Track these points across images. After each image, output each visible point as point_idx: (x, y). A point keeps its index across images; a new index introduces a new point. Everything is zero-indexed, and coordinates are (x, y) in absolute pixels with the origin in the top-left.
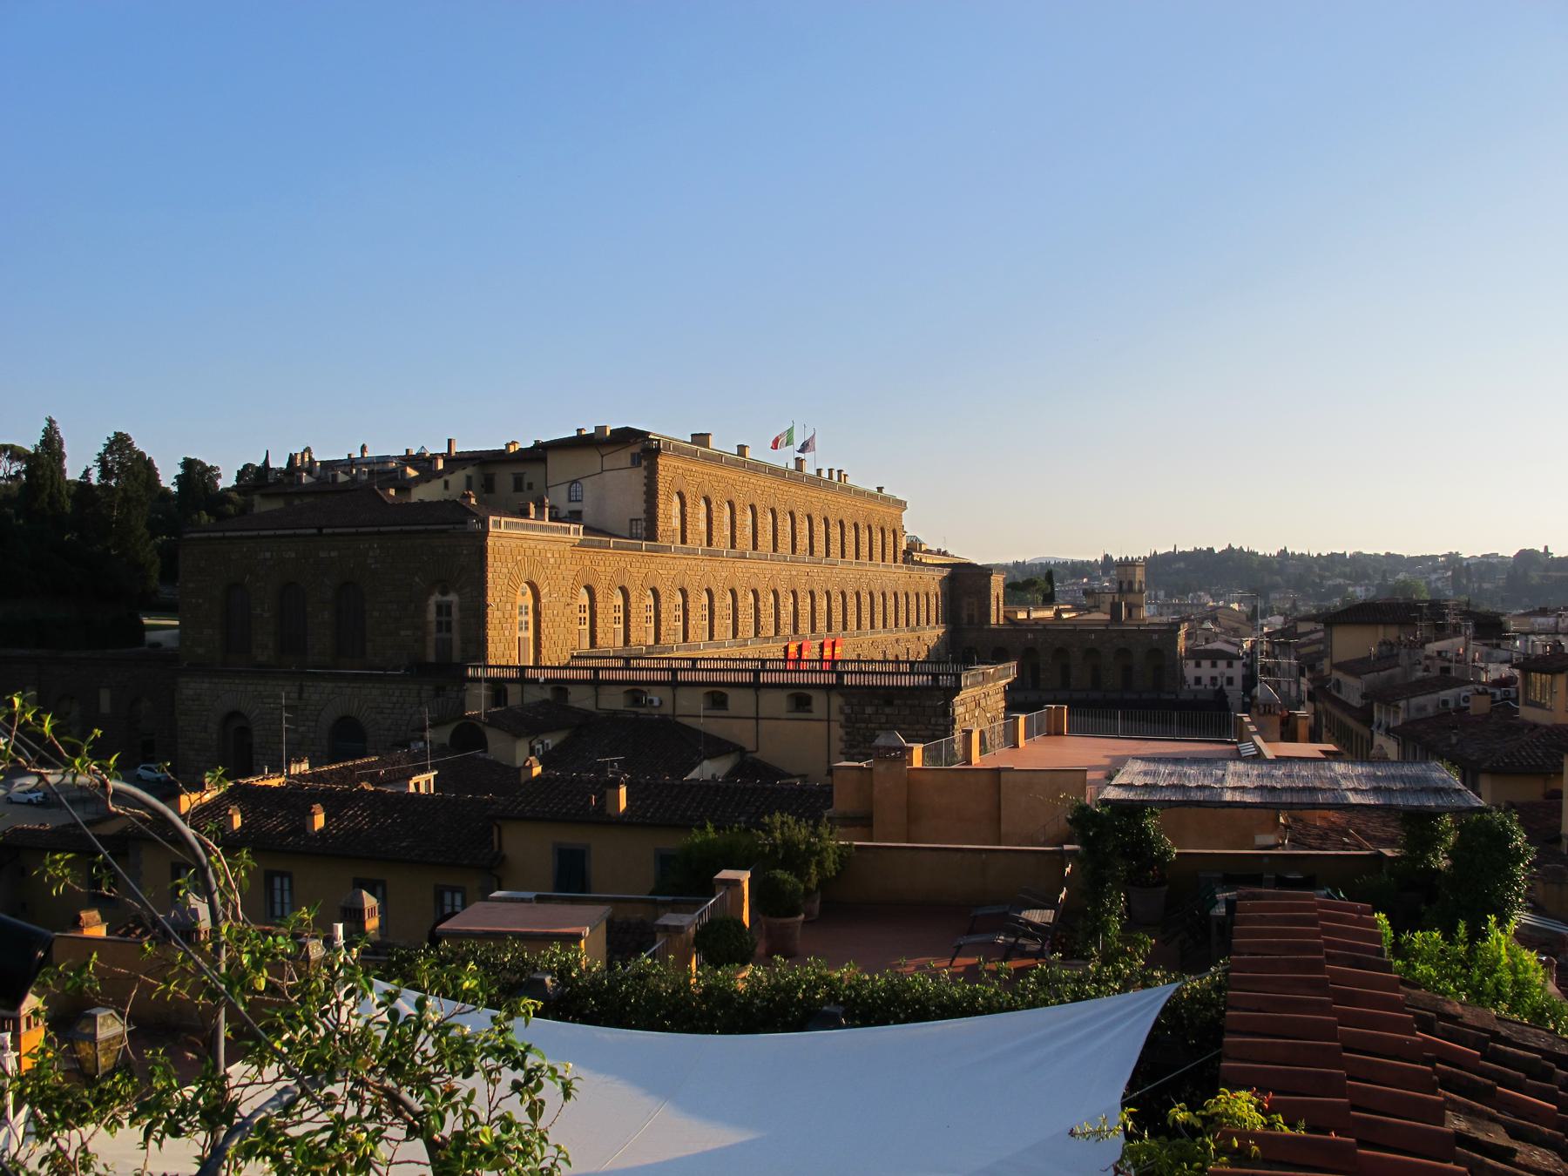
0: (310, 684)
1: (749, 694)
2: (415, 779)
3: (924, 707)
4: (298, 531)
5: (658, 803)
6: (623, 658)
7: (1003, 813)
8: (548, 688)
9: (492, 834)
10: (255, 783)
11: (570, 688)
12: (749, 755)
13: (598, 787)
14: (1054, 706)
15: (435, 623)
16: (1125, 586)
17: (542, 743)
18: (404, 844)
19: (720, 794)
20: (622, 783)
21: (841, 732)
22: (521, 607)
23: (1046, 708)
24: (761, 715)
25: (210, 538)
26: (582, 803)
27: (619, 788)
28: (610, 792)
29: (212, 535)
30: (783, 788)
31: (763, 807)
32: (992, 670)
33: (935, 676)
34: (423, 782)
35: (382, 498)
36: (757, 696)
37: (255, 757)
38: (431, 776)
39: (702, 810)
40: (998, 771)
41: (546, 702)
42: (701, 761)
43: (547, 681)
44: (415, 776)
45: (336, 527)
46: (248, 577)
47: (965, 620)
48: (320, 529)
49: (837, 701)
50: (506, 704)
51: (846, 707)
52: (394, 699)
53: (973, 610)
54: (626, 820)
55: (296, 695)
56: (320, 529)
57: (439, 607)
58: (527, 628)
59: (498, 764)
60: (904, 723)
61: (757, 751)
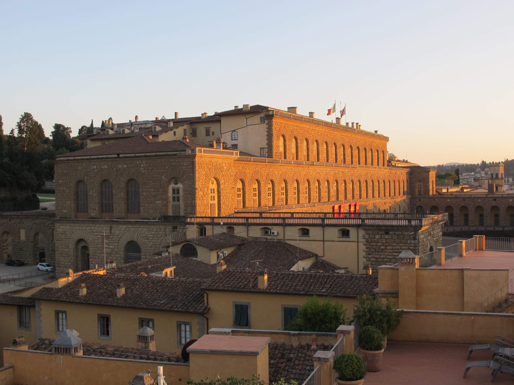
0: (115, 226)
1: (319, 230)
2: (166, 270)
3: (404, 235)
4: (108, 156)
5: (282, 283)
6: (259, 213)
7: (466, 291)
8: (225, 227)
9: (204, 297)
10: (92, 273)
11: (235, 227)
12: (320, 258)
13: (253, 275)
14: (478, 236)
15: (172, 198)
16: (494, 176)
17: (223, 253)
18: (162, 302)
19: (313, 278)
20: (265, 273)
21: (364, 247)
22: (211, 190)
23: (474, 237)
25: (68, 160)
26: (246, 283)
27: (264, 276)
28: (259, 277)
29: (69, 158)
30: (342, 276)
31: (334, 285)
32: (436, 217)
33: (410, 221)
34: (169, 271)
35: (146, 140)
36: (324, 230)
37: (90, 260)
38: (172, 269)
39: (304, 286)
40: (462, 270)
41: (224, 233)
42: (298, 261)
43: (224, 224)
44: (164, 269)
47: (417, 194)
48: (118, 155)
49: (362, 232)
50: (205, 235)
51: (366, 235)
52: (154, 233)
53: (421, 188)
54: (268, 291)
55: (109, 231)
56: (118, 155)
57: (174, 190)
58: (214, 199)
59: (203, 263)
60: (394, 243)
61: (323, 256)
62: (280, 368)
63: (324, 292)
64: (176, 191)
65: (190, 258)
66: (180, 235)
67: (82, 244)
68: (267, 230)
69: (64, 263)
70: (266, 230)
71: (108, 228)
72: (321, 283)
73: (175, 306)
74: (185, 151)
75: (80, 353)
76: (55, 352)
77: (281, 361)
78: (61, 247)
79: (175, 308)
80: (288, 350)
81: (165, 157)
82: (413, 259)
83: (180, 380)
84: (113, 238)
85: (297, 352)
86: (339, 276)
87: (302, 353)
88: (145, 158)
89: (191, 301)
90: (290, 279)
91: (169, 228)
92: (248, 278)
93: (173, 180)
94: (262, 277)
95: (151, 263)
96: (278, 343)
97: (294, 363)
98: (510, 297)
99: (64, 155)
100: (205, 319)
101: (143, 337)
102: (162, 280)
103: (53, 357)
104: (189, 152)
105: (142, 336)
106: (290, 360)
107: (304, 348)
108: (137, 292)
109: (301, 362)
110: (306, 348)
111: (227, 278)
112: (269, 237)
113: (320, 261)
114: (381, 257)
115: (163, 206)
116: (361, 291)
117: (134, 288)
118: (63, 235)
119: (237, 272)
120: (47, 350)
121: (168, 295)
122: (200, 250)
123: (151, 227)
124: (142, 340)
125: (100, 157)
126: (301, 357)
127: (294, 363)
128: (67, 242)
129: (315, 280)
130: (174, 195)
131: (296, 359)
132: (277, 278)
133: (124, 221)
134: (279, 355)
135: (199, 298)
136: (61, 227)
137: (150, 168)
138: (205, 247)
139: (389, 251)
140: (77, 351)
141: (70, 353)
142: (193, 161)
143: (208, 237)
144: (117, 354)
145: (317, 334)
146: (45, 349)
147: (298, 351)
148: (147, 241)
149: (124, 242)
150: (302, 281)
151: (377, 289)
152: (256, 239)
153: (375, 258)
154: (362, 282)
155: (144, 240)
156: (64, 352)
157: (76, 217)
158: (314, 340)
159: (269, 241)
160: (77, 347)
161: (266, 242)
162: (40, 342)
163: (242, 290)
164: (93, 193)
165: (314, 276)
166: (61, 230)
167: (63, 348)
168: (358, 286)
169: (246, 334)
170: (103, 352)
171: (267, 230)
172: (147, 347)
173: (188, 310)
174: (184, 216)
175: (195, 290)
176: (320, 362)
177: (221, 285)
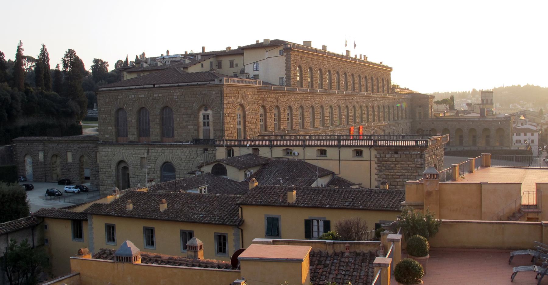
0: (152, 149)
3: (412, 154)
4: (145, 86)
6: (280, 136)
7: (483, 203)
8: (251, 149)
9: (239, 210)
11: (260, 149)
12: (336, 176)
13: (282, 191)
15: (203, 123)
16: (485, 102)
17: (250, 172)
18: (201, 216)
21: (376, 166)
25: (109, 90)
26: (276, 198)
27: (293, 192)
29: (110, 89)
30: (363, 191)
31: (355, 199)
32: (440, 138)
33: (416, 142)
40: (480, 184)
41: (250, 154)
42: (317, 178)
43: (250, 146)
46: (125, 106)
47: (418, 118)
48: (154, 85)
49: (374, 152)
50: (233, 155)
51: (378, 155)
52: (187, 154)
53: (421, 112)
54: (296, 205)
56: (154, 85)
57: (204, 116)
58: (240, 124)
59: (232, 181)
60: (403, 161)
62: (318, 273)
63: (347, 206)
64: (206, 117)
65: (221, 176)
66: (210, 156)
67: (123, 165)
69: (107, 182)
70: (288, 152)
71: (146, 151)
73: (213, 219)
74: (214, 81)
75: (139, 262)
76: (117, 260)
77: (319, 267)
80: (324, 257)
81: (196, 87)
82: (436, 175)
84: (150, 159)
85: (332, 259)
86: (360, 191)
87: (337, 260)
88: (178, 87)
89: (227, 214)
90: (315, 194)
91: (200, 150)
92: (278, 193)
93: (204, 107)
94: (292, 192)
95: (186, 181)
96: (315, 251)
97: (330, 269)
98: (522, 207)
100: (240, 230)
101: (190, 247)
102: (199, 196)
104: (216, 82)
105: (191, 246)
106: (326, 266)
107: (338, 256)
108: (178, 207)
109: (337, 268)
110: (340, 255)
111: (259, 193)
112: (290, 157)
114: (391, 174)
115: (195, 130)
116: (380, 204)
117: (175, 203)
118: (106, 157)
119: (268, 188)
120: (108, 259)
121: (206, 209)
122: (229, 169)
123: (184, 149)
124: (191, 249)
125: (137, 87)
126: (337, 263)
127: (330, 269)
129: (339, 195)
130: (205, 121)
131: (332, 265)
132: (304, 193)
133: (160, 144)
134: (317, 262)
135: (234, 211)
136: (104, 150)
137: (183, 97)
138: (234, 166)
139: (398, 168)
140: (136, 260)
141: (130, 261)
142: (221, 90)
143: (236, 157)
144: (172, 262)
145: (350, 242)
146: (106, 258)
147: (334, 258)
148: (180, 162)
149: (160, 162)
150: (326, 195)
151: (404, 202)
152: (279, 159)
154: (381, 196)
155: (178, 161)
156: (125, 261)
157: (117, 141)
158: (348, 248)
159: (291, 161)
160: (136, 256)
161: (288, 161)
162: (101, 252)
163: (273, 204)
164: (132, 119)
165: (338, 191)
166: (104, 153)
167: (124, 257)
168: (377, 200)
169: (286, 243)
170: (159, 261)
171: (288, 151)
172: (196, 256)
173: (225, 223)
175: (230, 205)
176: (380, 267)
177: (254, 200)
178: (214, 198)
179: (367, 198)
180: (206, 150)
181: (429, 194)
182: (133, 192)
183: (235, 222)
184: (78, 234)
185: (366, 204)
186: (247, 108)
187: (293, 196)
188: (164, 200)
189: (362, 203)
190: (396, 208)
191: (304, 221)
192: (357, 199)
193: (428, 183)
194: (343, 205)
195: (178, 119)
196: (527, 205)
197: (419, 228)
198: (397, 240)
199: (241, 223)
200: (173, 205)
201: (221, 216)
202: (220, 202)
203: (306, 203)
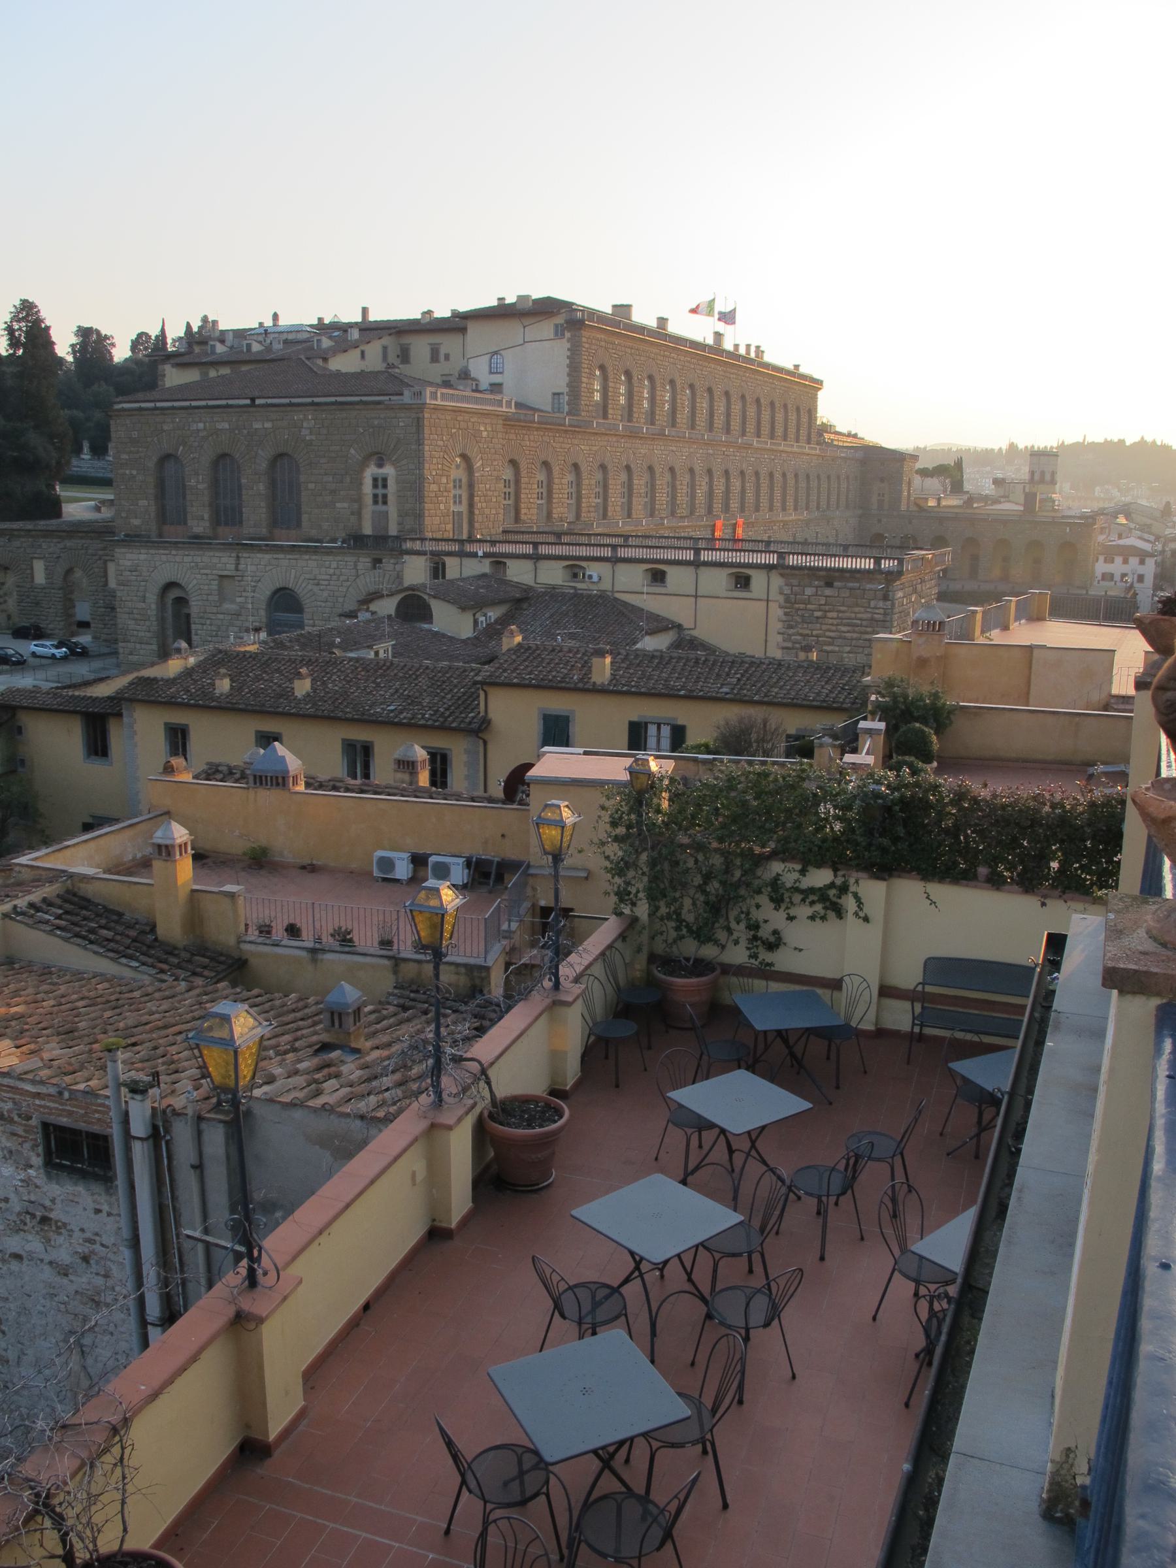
0: (247, 555)
3: (864, 590)
4: (231, 402)
6: (554, 534)
8: (487, 561)
11: (509, 562)
12: (687, 632)
13: (579, 656)
15: (371, 496)
16: (1037, 477)
17: (485, 615)
18: (392, 708)
21: (780, 612)
22: (455, 481)
24: (699, 594)
25: (141, 409)
26: (566, 671)
29: (144, 405)
33: (878, 561)
35: (311, 369)
37: (193, 627)
40: (1030, 648)
41: (484, 575)
42: (642, 636)
43: (486, 555)
45: (269, 398)
46: (181, 448)
48: (253, 400)
49: (777, 581)
50: (444, 577)
52: (332, 571)
55: (233, 567)
56: (253, 400)
57: (375, 480)
58: (460, 502)
59: (444, 635)
60: (843, 605)
63: (727, 693)
64: (380, 483)
65: (418, 625)
66: (387, 576)
67: (174, 594)
68: (576, 570)
69: (135, 632)
70: (575, 572)
71: (233, 560)
72: (718, 675)
73: (420, 716)
74: (402, 394)
75: (301, 788)
76: (255, 783)
78: (128, 598)
79: (420, 719)
81: (357, 407)
83: (503, 836)
84: (242, 581)
88: (311, 408)
89: (450, 706)
91: (365, 562)
92: (568, 661)
93: (376, 457)
95: (339, 632)
98: (1112, 701)
99: (130, 398)
100: (481, 742)
102: (384, 665)
103: (251, 793)
104: (407, 398)
108: (336, 688)
111: (525, 661)
112: (579, 585)
113: (688, 638)
114: (815, 633)
115: (352, 513)
116: (801, 692)
117: (329, 679)
118: (134, 573)
119: (545, 649)
121: (402, 694)
122: (437, 607)
123: (325, 558)
125: (211, 403)
128: (142, 589)
130: (384, 491)
133: (267, 545)
135: (466, 700)
136: (129, 556)
137: (325, 431)
138: (448, 602)
139: (831, 621)
141: (284, 785)
142: (418, 418)
143: (452, 581)
148: (316, 589)
149: (265, 591)
150: (679, 669)
151: (869, 678)
152: (554, 588)
153: (801, 635)
155: (310, 587)
156: (272, 785)
157: (160, 535)
159: (582, 594)
161: (575, 595)
162: (210, 769)
163: (560, 685)
164: (198, 483)
166: (129, 563)
167: (271, 777)
171: (576, 570)
173: (447, 724)
174: (397, 537)
175: (456, 686)
177: (514, 675)
178: (418, 670)
179: (770, 677)
180: (377, 562)
181: (922, 662)
182: (226, 652)
183: (470, 723)
184: (98, 747)
185: (769, 691)
186: (478, 465)
187: (603, 669)
188: (304, 671)
189: (760, 688)
190: (834, 702)
191: (626, 726)
192: (748, 679)
193: (921, 640)
194: (718, 693)
195: (311, 486)
196: (1123, 697)
197: (916, 714)
198: (878, 731)
199: (484, 726)
200: (324, 683)
201: (437, 711)
202: (432, 678)
203: (633, 683)
